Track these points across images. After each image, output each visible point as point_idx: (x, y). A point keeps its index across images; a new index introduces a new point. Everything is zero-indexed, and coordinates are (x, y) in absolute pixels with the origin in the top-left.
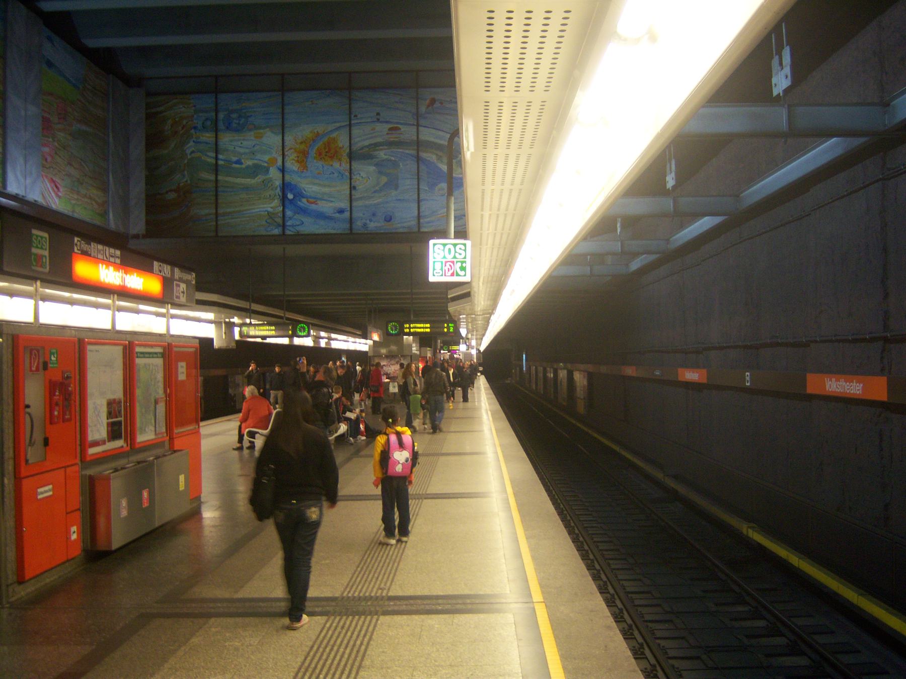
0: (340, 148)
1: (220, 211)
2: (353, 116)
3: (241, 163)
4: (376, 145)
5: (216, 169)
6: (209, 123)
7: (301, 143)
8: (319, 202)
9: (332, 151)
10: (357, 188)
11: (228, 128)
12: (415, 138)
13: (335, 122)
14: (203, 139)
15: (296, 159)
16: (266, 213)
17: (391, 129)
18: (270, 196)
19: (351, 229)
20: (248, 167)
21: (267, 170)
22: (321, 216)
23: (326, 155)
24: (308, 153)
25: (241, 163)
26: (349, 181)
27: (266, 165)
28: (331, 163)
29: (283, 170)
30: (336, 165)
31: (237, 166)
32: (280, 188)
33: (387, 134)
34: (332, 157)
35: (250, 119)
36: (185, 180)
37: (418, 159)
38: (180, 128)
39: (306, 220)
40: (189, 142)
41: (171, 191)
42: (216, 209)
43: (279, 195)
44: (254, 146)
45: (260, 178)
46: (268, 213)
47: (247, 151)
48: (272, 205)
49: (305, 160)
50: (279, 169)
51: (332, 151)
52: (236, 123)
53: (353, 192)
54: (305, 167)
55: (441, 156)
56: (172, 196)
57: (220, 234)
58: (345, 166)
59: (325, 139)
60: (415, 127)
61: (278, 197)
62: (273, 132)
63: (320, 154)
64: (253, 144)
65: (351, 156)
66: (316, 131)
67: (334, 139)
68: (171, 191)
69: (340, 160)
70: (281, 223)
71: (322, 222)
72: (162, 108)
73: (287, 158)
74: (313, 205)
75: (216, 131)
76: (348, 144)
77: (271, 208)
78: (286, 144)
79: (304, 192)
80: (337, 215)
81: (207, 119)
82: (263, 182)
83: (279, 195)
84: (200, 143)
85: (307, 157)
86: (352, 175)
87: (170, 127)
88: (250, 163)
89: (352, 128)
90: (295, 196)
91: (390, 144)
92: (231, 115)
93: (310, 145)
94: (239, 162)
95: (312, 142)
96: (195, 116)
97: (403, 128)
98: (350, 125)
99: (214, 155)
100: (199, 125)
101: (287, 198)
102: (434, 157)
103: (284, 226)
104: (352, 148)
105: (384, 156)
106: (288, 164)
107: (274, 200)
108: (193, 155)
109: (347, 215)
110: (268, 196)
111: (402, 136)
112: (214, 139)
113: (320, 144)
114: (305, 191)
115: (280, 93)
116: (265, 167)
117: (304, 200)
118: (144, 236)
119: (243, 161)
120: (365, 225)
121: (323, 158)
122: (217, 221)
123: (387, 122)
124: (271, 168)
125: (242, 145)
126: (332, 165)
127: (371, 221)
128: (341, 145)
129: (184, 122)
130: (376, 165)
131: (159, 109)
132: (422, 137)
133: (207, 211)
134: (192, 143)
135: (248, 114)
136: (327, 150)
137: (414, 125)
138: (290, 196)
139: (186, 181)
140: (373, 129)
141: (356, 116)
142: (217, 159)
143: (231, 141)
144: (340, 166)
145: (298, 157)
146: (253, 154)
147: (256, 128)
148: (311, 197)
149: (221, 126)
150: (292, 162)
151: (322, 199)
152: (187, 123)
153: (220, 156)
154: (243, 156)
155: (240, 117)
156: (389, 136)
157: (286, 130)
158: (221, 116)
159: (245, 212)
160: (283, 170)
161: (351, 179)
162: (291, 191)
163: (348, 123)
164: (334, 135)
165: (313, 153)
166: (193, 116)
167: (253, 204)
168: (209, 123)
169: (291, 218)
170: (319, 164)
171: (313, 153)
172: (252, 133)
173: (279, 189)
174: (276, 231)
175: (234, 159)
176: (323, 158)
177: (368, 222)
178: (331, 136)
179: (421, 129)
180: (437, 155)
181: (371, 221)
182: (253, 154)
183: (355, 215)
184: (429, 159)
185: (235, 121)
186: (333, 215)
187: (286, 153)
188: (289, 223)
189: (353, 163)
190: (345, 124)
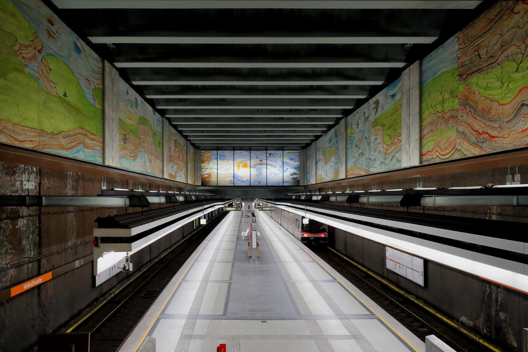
4: (256, 164)
6: (215, 158)
9: (246, 166)
13: (247, 158)
14: (214, 162)
21: (230, 170)
22: (243, 181)
30: (247, 168)
31: (223, 169)
35: (226, 157)
39: (239, 182)
51: (246, 166)
56: (206, 175)
57: (218, 185)
59: (244, 163)
63: (243, 166)
68: (206, 174)
71: (243, 183)
72: (203, 154)
80: (247, 181)
81: (215, 157)
94: (223, 168)
100: (213, 158)
102: (271, 167)
103: (234, 184)
108: (212, 166)
113: (243, 164)
115: (233, 151)
118: (201, 186)
130: (257, 169)
131: (203, 154)
133: (215, 180)
134: (211, 163)
138: (235, 176)
147: (227, 159)
149: (218, 158)
155: (223, 156)
158: (218, 156)
162: (236, 175)
164: (246, 162)
165: (241, 166)
168: (215, 158)
169: (235, 182)
171: (241, 166)
172: (226, 161)
174: (232, 185)
175: (222, 167)
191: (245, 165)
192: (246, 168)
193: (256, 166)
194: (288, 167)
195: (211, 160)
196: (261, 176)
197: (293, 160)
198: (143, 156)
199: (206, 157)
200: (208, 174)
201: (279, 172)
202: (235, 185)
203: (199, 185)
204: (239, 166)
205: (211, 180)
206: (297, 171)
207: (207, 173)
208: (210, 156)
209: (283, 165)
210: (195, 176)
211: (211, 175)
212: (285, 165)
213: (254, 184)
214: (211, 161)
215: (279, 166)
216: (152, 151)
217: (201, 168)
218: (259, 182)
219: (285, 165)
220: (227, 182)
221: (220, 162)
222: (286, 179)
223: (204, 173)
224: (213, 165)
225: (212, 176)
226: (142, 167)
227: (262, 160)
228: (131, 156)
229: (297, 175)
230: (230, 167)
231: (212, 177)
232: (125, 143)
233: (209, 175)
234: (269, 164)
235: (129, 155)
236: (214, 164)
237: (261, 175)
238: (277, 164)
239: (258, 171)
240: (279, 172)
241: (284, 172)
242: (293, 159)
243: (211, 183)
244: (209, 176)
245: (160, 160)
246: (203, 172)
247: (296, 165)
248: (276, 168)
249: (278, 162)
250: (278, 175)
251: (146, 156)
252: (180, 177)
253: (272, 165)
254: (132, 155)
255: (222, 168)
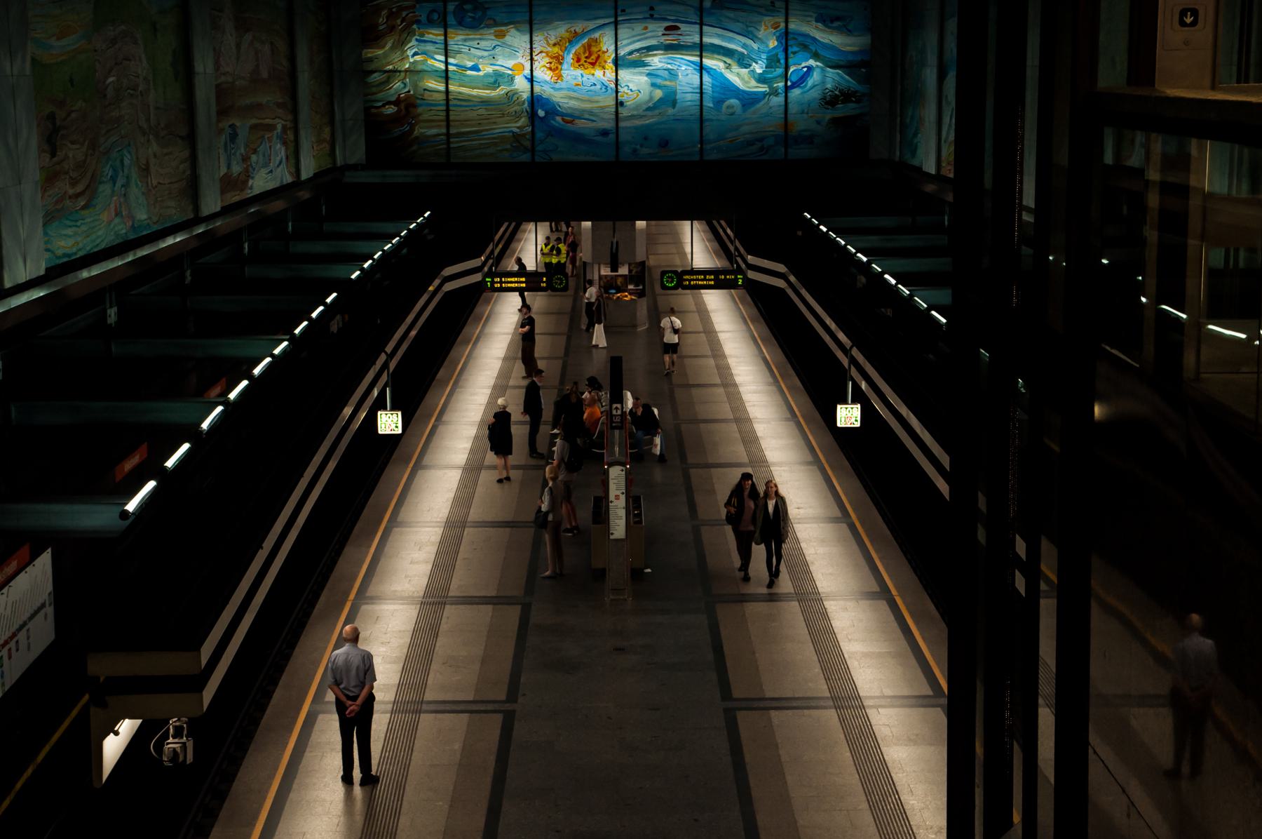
0: (604, 52)
1: (453, 131)
2: (619, 12)
3: (479, 70)
5: (446, 76)
6: (435, 16)
7: (555, 45)
8: (577, 121)
9: (593, 57)
10: (625, 104)
11: (461, 24)
12: (697, 39)
13: (596, 18)
15: (548, 65)
16: (511, 134)
17: (667, 29)
18: (516, 112)
19: (617, 155)
20: (487, 75)
21: (512, 79)
22: (578, 138)
23: (585, 61)
24: (563, 59)
25: (479, 70)
26: (614, 95)
27: (510, 72)
28: (593, 72)
29: (531, 80)
30: (598, 73)
32: (529, 103)
33: (663, 35)
34: (593, 64)
35: (489, 13)
36: (407, 90)
37: (701, 68)
38: (399, 21)
40: (410, 41)
41: (389, 103)
42: (448, 126)
43: (527, 111)
44: (495, 47)
45: (502, 90)
46: (514, 135)
47: (486, 54)
48: (518, 125)
49: (560, 67)
50: (526, 78)
51: (593, 57)
52: (471, 17)
53: (620, 109)
54: (560, 77)
55: (730, 64)
56: (391, 110)
58: (610, 74)
60: (698, 26)
61: (526, 114)
62: (518, 30)
63: (578, 60)
64: (493, 45)
65: (616, 63)
66: (573, 29)
67: (596, 41)
68: (389, 103)
69: (604, 68)
70: (530, 147)
73: (536, 64)
74: (569, 125)
75: (445, 27)
76: (613, 47)
77: (518, 128)
78: (534, 46)
79: (559, 108)
80: (599, 138)
81: (433, 11)
82: (507, 94)
83: (527, 111)
84: (425, 41)
85: (561, 64)
86: (619, 87)
87: (385, 20)
88: (489, 69)
89: (618, 27)
90: (547, 113)
91: (669, 48)
92: (465, 7)
93: (566, 48)
94: (475, 68)
95: (567, 44)
96: (418, 6)
97: (683, 27)
98: (616, 24)
99: (442, 58)
100: (423, 18)
101: (537, 115)
102: (721, 65)
103: (533, 151)
104: (619, 52)
105: (658, 64)
106: (538, 74)
107: (521, 117)
108: (418, 58)
109: (612, 137)
110: (514, 113)
111: (681, 37)
112: (443, 38)
114: (560, 106)
116: (509, 75)
117: (559, 119)
119: (480, 66)
120: (635, 151)
121: (583, 65)
122: (448, 142)
123: (665, 19)
124: (516, 77)
125: (478, 46)
126: (593, 75)
127: (642, 146)
128: (604, 49)
129: (404, 14)
130: (648, 75)
132: (706, 40)
133: (434, 131)
134: (413, 42)
135: (486, 6)
136: (587, 55)
137: (695, 23)
138: (541, 113)
139: (409, 91)
140: (646, 28)
141: (623, 11)
142: (447, 63)
143: (465, 40)
144: (604, 75)
145: (551, 63)
146: (494, 58)
147: (496, 24)
148: (567, 115)
149: (451, 20)
150: (542, 69)
151: (579, 118)
152: (407, 15)
153: (451, 60)
154: (481, 60)
156: (666, 37)
157: (535, 27)
159: (483, 133)
160: (531, 80)
161: (617, 92)
162: (542, 108)
163: (612, 20)
164: (597, 35)
165: (569, 58)
166: (414, 7)
167: (494, 123)
170: (579, 72)
171: (569, 58)
173: (526, 105)
174: (525, 158)
175: (470, 64)
176: (583, 65)
177: (638, 147)
178: (593, 37)
179: (705, 28)
180: (725, 62)
181: (642, 146)
182: (494, 58)
183: (622, 137)
184: (714, 67)
185: (470, 14)
186: (595, 138)
187: (535, 58)
188: (539, 148)
189: (620, 72)
190: (607, 21)
191: (590, 54)
192: (597, 67)
193: (648, 59)
194: (812, 62)
195: (415, 26)
196: (671, 111)
197: (836, 24)
198: (118, 163)
199: (384, 12)
200: (397, 102)
201: (763, 88)
202: (537, 159)
203: (352, 161)
204: (559, 59)
205: (416, 133)
206: (859, 82)
207: (393, 99)
208: (406, 8)
209: (786, 50)
210: (332, 122)
211: (415, 106)
212: (795, 49)
213: (635, 151)
214: (412, 33)
215: (764, 56)
216: (148, 120)
217: (363, 71)
218: (664, 144)
219: (794, 53)
220: (496, 144)
221: (457, 39)
222: (801, 124)
223: (380, 96)
224: (424, 53)
225: (420, 110)
226: (117, 215)
227: (677, 28)
228: (78, 195)
229: (858, 102)
230: (510, 63)
231: (425, 116)
232: (53, 155)
233: (408, 105)
234: (713, 45)
235: (71, 192)
236: (430, 47)
237: (674, 103)
238: (755, 46)
239: (653, 85)
240: (763, 88)
241: (794, 85)
242: (838, 19)
243: (415, 148)
244: (404, 112)
245: (182, 138)
246: (374, 90)
247: (849, 49)
248: (747, 66)
249: (761, 33)
250: (758, 106)
251: (127, 162)
252: (266, 165)
253: (728, 53)
254: (80, 188)
255: (469, 72)
